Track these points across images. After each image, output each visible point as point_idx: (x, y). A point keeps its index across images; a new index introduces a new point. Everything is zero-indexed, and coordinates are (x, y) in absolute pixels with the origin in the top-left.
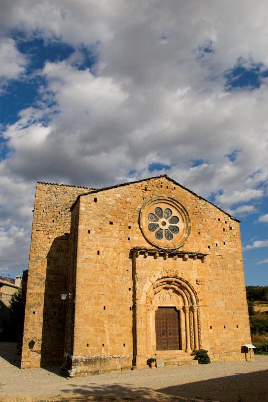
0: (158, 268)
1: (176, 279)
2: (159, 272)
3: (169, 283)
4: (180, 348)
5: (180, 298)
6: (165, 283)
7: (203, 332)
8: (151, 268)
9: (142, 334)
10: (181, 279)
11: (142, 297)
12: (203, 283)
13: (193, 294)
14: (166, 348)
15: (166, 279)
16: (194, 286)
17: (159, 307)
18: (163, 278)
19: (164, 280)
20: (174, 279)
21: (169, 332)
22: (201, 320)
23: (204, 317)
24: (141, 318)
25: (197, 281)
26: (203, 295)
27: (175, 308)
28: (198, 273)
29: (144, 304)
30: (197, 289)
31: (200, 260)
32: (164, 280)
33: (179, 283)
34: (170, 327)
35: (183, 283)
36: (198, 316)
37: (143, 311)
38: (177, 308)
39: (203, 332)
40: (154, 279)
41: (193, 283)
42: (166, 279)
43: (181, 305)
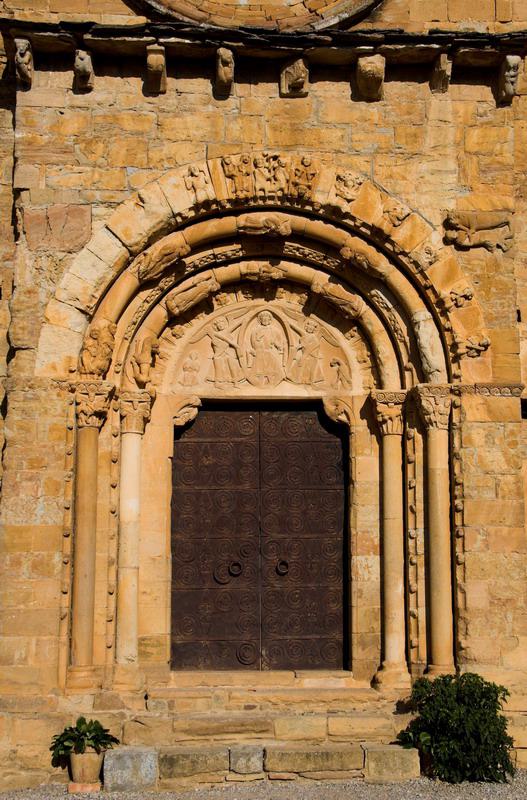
0: (168, 149)
1: (302, 222)
2: (177, 177)
3: (266, 245)
4: (346, 664)
5: (350, 345)
6: (228, 250)
7: (485, 557)
8: (119, 149)
9: (35, 567)
10: (334, 215)
11: (46, 333)
12: (492, 237)
13: (421, 314)
14: (249, 656)
15: (229, 223)
16: (424, 260)
17: (208, 405)
18: (207, 210)
19: (212, 227)
20: (285, 222)
21: (274, 558)
22: (470, 478)
23: (495, 458)
24: (37, 464)
25: (448, 225)
26: (489, 319)
27: (316, 405)
28: (462, 171)
29: (62, 374)
30: (450, 276)
31: (484, 92)
32: (212, 227)
33: (330, 248)
34: (284, 524)
35: (356, 246)
36: (452, 456)
37: (50, 420)
38: (330, 408)
39: (485, 557)
40: (139, 225)
41: (424, 240)
42: (229, 223)
43: (359, 385)
